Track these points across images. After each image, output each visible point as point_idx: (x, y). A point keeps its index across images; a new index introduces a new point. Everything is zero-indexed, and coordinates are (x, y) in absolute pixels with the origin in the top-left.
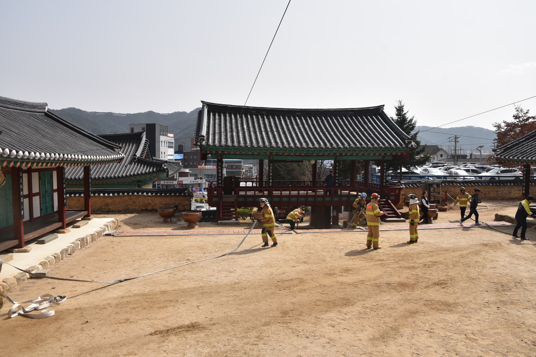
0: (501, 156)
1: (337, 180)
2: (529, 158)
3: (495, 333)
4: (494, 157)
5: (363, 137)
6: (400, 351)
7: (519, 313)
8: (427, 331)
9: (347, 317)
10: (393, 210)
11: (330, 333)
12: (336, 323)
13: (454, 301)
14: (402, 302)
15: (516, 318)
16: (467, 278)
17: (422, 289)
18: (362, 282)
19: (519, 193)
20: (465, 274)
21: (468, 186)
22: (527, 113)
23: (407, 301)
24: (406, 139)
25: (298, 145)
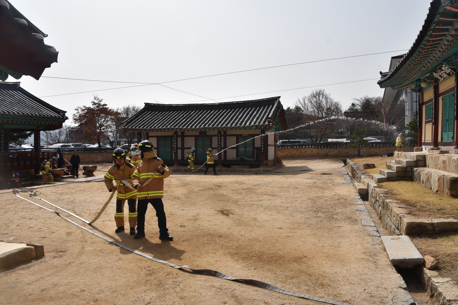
4: (121, 128)
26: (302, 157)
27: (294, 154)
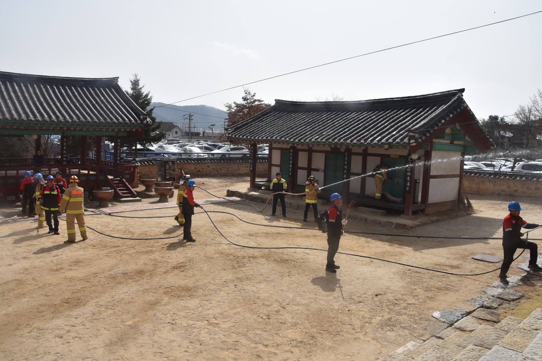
0: (232, 135)
1: (65, 157)
2: (256, 138)
3: (235, 313)
5: (95, 111)
6: (141, 353)
7: (255, 288)
8: (169, 323)
9: (78, 321)
10: (128, 189)
11: (57, 346)
12: (65, 331)
13: (194, 285)
14: (141, 292)
15: (251, 293)
16: (205, 257)
17: (161, 275)
18: (95, 275)
19: (246, 170)
20: (203, 254)
21: (202, 163)
22: (254, 96)
23: (146, 291)
24: (141, 115)
25: (16, 116)
26: (530, 196)
27: (516, 191)
